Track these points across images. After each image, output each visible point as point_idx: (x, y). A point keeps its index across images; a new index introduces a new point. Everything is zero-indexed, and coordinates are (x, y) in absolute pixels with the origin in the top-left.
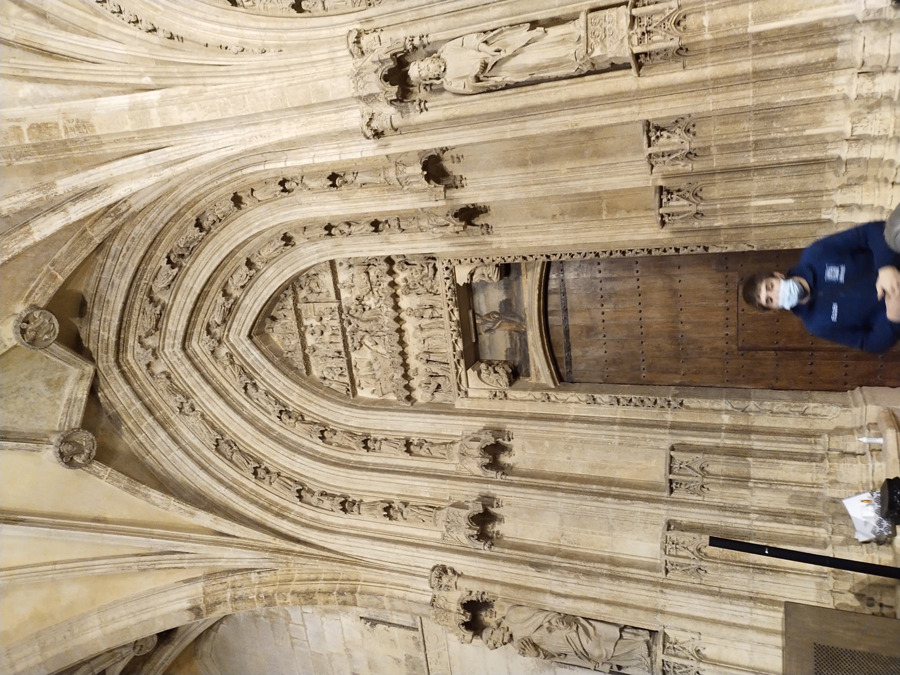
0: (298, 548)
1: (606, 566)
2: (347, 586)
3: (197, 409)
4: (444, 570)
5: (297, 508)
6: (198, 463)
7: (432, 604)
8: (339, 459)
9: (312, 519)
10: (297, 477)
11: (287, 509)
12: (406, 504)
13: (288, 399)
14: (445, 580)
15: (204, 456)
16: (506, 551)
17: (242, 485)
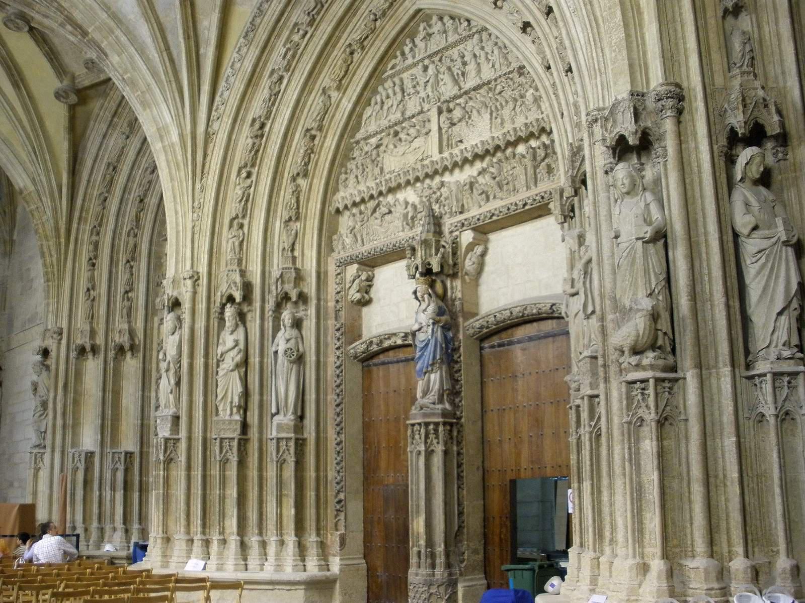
0: (63, 240)
1: (71, 422)
2: (50, 276)
3: (128, 141)
4: (61, 334)
5: (88, 228)
6: (97, 155)
7: (47, 330)
8: (119, 245)
9: (83, 240)
10: (104, 221)
11: (86, 222)
12: (93, 300)
13: (152, 196)
14: (55, 336)
15: (103, 156)
16: (74, 367)
17: (94, 186)
